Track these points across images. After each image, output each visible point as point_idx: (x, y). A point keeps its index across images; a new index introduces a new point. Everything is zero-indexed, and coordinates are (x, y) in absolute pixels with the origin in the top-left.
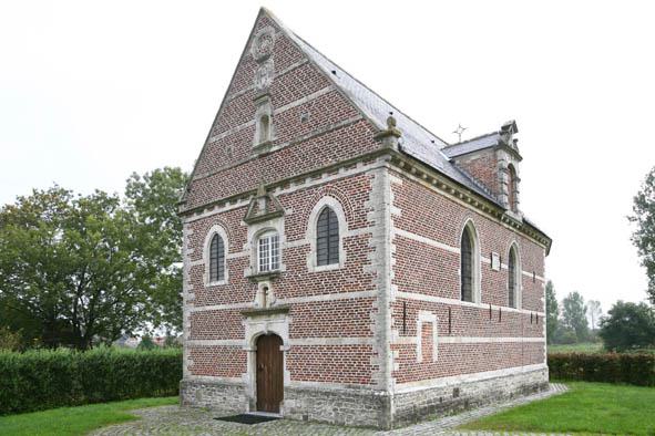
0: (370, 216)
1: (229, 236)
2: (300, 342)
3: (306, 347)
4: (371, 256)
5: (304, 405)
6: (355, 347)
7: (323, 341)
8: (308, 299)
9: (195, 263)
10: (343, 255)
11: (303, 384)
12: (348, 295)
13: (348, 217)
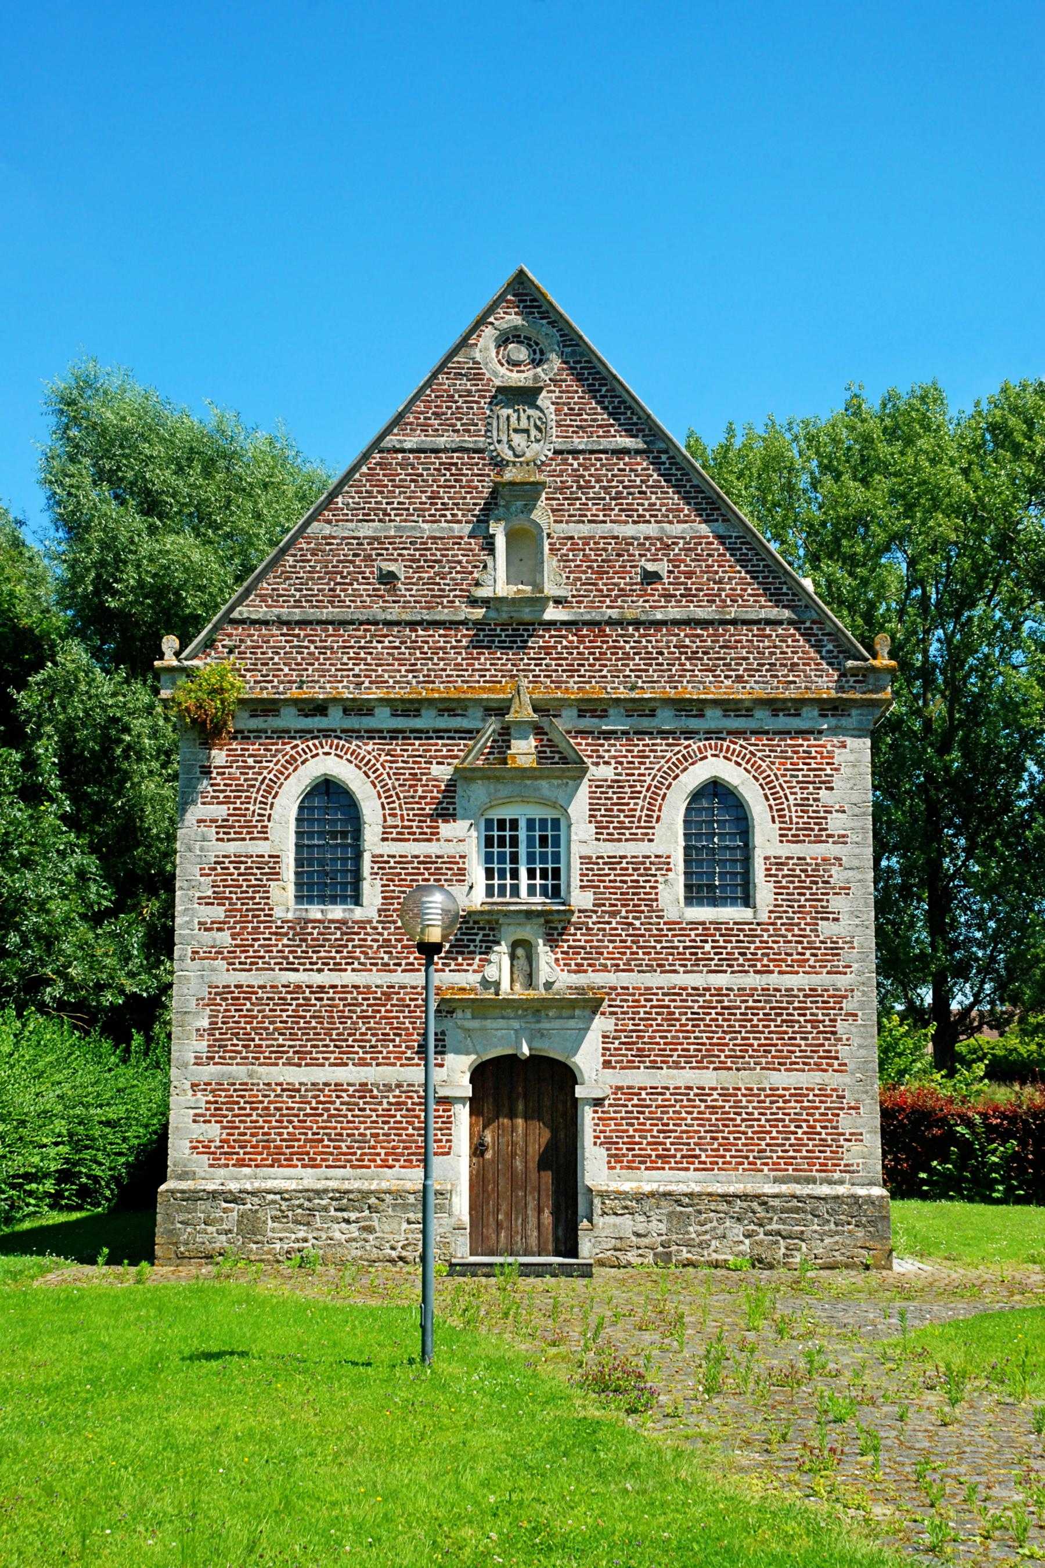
0: (836, 823)
1: (386, 794)
2: (640, 1077)
3: (654, 1091)
4: (837, 903)
5: (658, 1227)
6: (799, 1094)
7: (709, 1078)
8: (657, 980)
9: (232, 848)
10: (764, 892)
11: (648, 1181)
12: (774, 980)
13: (778, 814)
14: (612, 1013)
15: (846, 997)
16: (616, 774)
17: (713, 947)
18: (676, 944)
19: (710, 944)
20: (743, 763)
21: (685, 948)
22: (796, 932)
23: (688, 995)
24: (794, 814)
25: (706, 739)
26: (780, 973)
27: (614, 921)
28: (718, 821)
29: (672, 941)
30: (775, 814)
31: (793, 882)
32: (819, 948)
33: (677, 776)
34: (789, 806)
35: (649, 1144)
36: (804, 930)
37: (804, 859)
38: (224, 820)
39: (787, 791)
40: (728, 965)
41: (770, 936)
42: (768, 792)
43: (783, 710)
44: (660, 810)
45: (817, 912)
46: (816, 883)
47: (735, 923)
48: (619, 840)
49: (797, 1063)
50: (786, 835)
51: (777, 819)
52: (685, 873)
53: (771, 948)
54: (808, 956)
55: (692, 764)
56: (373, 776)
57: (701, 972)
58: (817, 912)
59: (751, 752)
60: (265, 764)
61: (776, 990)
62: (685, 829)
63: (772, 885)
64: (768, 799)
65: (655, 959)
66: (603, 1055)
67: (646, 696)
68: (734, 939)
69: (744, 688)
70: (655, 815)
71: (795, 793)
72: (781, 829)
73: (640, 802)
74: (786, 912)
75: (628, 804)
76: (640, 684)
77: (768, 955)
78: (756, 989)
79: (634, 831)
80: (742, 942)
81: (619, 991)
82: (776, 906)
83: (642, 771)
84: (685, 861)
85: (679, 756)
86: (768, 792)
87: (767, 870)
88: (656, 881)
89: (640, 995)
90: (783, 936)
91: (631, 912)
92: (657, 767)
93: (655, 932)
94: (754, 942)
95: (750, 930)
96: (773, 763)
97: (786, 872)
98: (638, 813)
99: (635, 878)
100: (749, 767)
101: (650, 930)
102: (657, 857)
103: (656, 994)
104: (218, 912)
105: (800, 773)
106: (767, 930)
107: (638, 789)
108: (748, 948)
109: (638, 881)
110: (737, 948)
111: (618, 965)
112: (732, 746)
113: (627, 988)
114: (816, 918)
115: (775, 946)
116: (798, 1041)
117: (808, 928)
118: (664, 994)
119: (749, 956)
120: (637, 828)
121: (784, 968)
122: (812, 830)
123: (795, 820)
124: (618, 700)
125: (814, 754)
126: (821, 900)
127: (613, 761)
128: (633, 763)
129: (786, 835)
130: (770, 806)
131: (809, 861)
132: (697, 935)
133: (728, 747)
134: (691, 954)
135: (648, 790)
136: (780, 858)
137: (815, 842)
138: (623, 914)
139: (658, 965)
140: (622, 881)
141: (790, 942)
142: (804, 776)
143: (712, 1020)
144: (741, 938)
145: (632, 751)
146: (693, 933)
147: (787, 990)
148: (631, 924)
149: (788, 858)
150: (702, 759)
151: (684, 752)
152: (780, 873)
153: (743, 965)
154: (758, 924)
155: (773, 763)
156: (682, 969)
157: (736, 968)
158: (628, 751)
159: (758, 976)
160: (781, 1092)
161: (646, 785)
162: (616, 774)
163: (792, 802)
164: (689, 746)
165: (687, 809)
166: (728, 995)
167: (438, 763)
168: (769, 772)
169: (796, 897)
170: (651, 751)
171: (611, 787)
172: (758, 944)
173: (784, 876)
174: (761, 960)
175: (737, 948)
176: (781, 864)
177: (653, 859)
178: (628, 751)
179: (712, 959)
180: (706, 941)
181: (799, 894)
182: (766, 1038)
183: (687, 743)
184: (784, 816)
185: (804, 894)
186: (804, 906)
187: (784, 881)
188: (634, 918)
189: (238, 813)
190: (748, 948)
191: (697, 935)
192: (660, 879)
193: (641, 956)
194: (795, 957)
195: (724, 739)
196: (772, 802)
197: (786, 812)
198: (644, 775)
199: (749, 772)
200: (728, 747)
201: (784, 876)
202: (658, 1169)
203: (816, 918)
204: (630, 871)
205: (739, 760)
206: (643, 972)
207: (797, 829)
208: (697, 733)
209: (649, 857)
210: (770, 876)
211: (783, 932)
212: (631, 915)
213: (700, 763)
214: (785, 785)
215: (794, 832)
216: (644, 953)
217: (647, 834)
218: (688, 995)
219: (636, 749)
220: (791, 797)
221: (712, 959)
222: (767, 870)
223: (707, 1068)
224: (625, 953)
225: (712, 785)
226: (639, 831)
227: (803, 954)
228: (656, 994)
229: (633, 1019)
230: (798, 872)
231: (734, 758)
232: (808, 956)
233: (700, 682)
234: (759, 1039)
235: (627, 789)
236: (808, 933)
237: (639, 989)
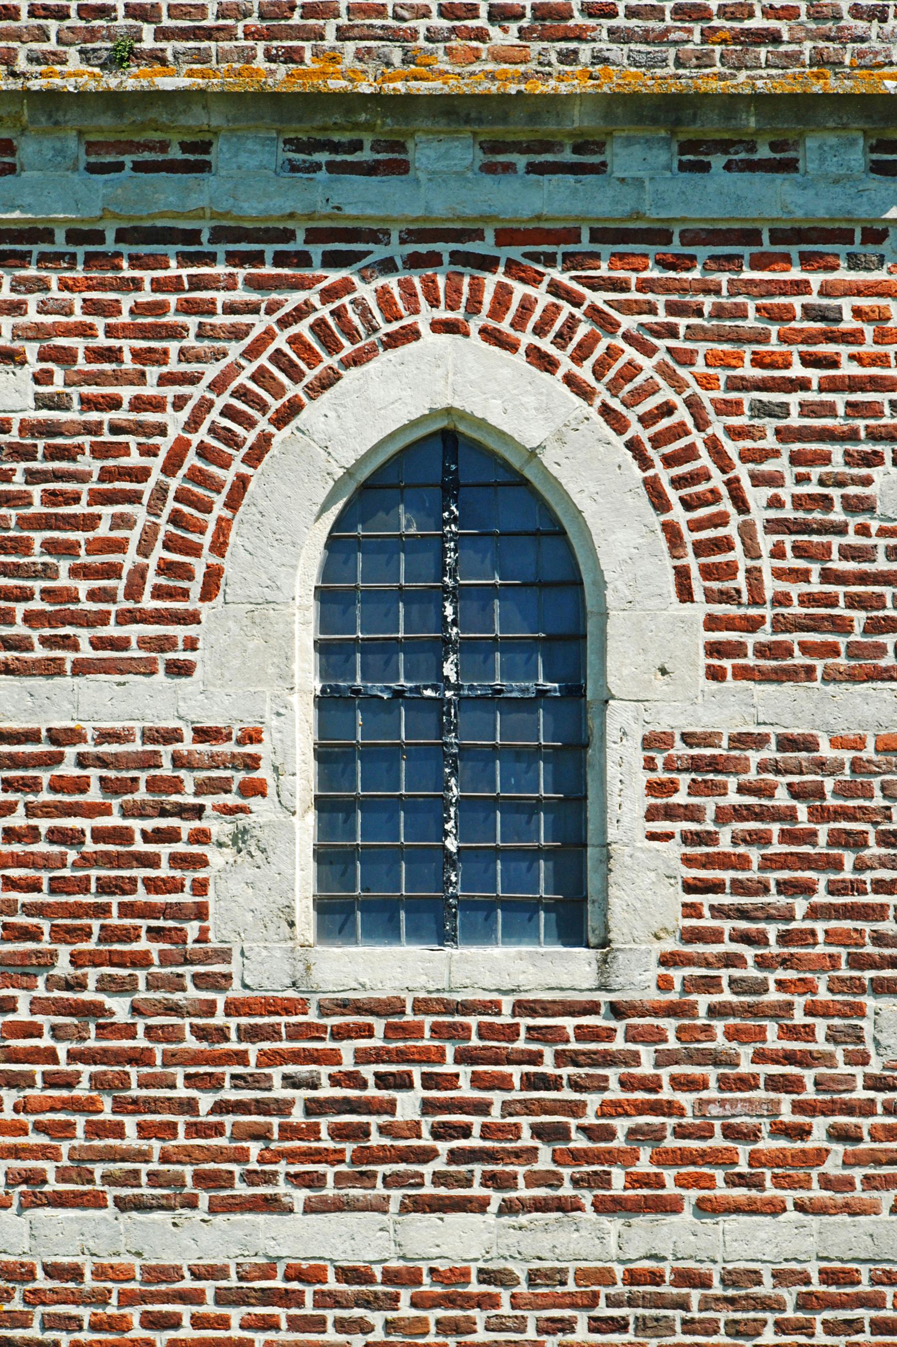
16: (43, 402)
17: (428, 1107)
18: (280, 1092)
19: (420, 1092)
20: (563, 357)
21: (314, 1108)
22: (773, 1042)
23: (325, 1300)
24: (766, 564)
25: (415, 262)
26: (705, 1208)
27: (23, 999)
28: (458, 594)
29: (265, 1084)
30: (692, 562)
31: (760, 839)
32: (866, 1109)
33: (293, 409)
34: (747, 531)
36: (807, 1033)
37: (808, 744)
39: (742, 471)
40: (490, 1180)
41: (664, 1059)
42: (664, 475)
43: (724, 146)
44: (219, 547)
45: (856, 962)
46: (856, 842)
47: (523, 1008)
48: (52, 669)
50: (736, 650)
51: (698, 584)
52: (321, 804)
53: (670, 1109)
54: (818, 1139)
55: (355, 361)
57: (380, 1206)
58: (856, 962)
59: (594, 313)
61: (686, 1278)
62: (325, 624)
63: (674, 850)
64: (660, 503)
65: (188, 1155)
67: (167, 83)
68: (516, 1072)
69: (569, 57)
70: (199, 567)
71: (774, 480)
72: (712, 623)
73: (139, 512)
74: (732, 961)
75: (90, 523)
76: (148, 43)
77: (654, 1135)
78: (605, 1277)
79: (111, 630)
80: (550, 1083)
81: (42, 1282)
82: (691, 936)
83: (150, 390)
84: (322, 755)
85: (303, 328)
86: (664, 475)
87: (654, 788)
88: (200, 837)
89: (127, 1299)
90: (715, 1059)
91: (95, 960)
92: (212, 371)
93: (191, 1043)
94: (601, 1085)
95: (583, 1034)
96: (685, 358)
97: (733, 798)
98: (129, 560)
99: (114, 820)
100: (585, 372)
101: (171, 1035)
102: (203, 734)
103: (194, 1297)
105: (794, 399)
106: (656, 1036)
107: (134, 460)
108: (575, 1109)
109: (122, 836)
110: (528, 1108)
111: (35, 1178)
112: (520, 290)
113: (75, 1273)
114: (855, 986)
115: (686, 1099)
117: (821, 1026)
118: (222, 1298)
119: (579, 1142)
120: (127, 618)
121: (722, 1191)
122: (842, 626)
123: (771, 586)
124: (52, 96)
125: (849, 323)
127: (31, 350)
128: (113, 355)
129: (737, 650)
130: (672, 532)
131: (826, 751)
132: (362, 1057)
133: (503, 294)
134: (339, 1133)
135: (170, 468)
136: (707, 740)
137: (852, 677)
138: (63, 968)
139: (200, 1179)
140: (58, 836)
141: (746, 1083)
142: (807, 409)
144: (548, 1067)
145: (110, 309)
146: (347, 1048)
147: (730, 1279)
148: (97, 1010)
149: (741, 741)
150: (393, 341)
151: (324, 312)
152: (710, 804)
153: (551, 1180)
154: (617, 1011)
156: (300, 1196)
157: (523, 1192)
158: (91, 307)
159: (613, 1225)
161: (164, 444)
162: (43, 402)
163: (759, 515)
164: (346, 287)
165: (332, 543)
166: (487, 1302)
168: (666, 394)
169: (774, 898)
170: (189, 308)
171: (27, 454)
172: (615, 1093)
173: (723, 816)
174: (627, 1158)
175: (528, 1108)
176: (715, 765)
177: (187, 746)
178: (91, 307)
179: (427, 1155)
180: (404, 1083)
181: (786, 888)
183: (334, 276)
184: (730, 570)
185: (807, 889)
186: (806, 937)
187: (725, 835)
188: (107, 985)
190: (575, 1109)
191: (362, 1057)
192: (218, 827)
193: (132, 1140)
194: (768, 1144)
195: (488, 264)
196: (679, 515)
197: (737, 554)
198: (157, 405)
199: (584, 392)
200: (503, 294)
201: (723, 816)
203: (855, 986)
204: (94, 795)
205: (545, 344)
206: (139, 1205)
207: (781, 625)
208: (376, 236)
209: (173, 736)
210: (670, 813)
211: (721, 1043)
212: (92, 974)
213: (386, 357)
214: (731, 448)
215: (765, 635)
216: (144, 1130)
217: (164, 644)
218: (325, 1300)
219: (127, 301)
220: (756, 496)
221: (427, 1155)
222: (654, 788)
224: (66, 1131)
225: (437, 446)
226: (134, 631)
227: (803, 1132)
228: (194, 1297)
230: (782, 799)
231: (527, 338)
232: (818, 1139)
233: (391, 35)
235: (87, 463)
236: (821, 1045)
237: (122, 1275)
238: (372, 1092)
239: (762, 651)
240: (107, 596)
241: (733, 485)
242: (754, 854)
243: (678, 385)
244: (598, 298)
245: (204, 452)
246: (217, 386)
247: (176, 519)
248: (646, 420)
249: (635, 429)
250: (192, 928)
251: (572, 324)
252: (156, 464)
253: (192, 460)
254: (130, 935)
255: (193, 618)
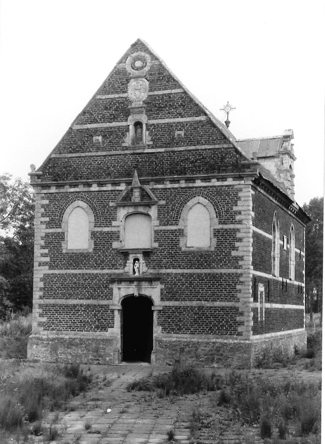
14: (164, 282)
15: (240, 276)
31: (223, 238)
35: (175, 325)
38: (48, 222)
49: (223, 299)
56: (92, 207)
59: (210, 194)
60: (60, 204)
66: (161, 296)
72: (219, 220)
104: (46, 251)
116: (224, 291)
126: (232, 244)
135: (177, 208)
143: (196, 284)
146: (190, 256)
155: (217, 197)
160: (217, 308)
161: (176, 206)
167: (112, 202)
168: (216, 200)
182: (213, 290)
189: (52, 220)
202: (177, 333)
207: (225, 219)
214: (221, 205)
223: (194, 300)
229: (171, 284)
234: (211, 291)
238: (192, 259)
239: (223, 222)
240: (172, 219)
241: (221, 208)
242: (222, 239)
243: (217, 200)
244: (210, 193)
245: (179, 207)
246: (180, 201)
247: (177, 212)
248: (214, 203)
249: (213, 203)
250: (178, 246)
251: (208, 195)
252: (175, 208)
253: (178, 207)
254: (173, 247)
255: (178, 220)
